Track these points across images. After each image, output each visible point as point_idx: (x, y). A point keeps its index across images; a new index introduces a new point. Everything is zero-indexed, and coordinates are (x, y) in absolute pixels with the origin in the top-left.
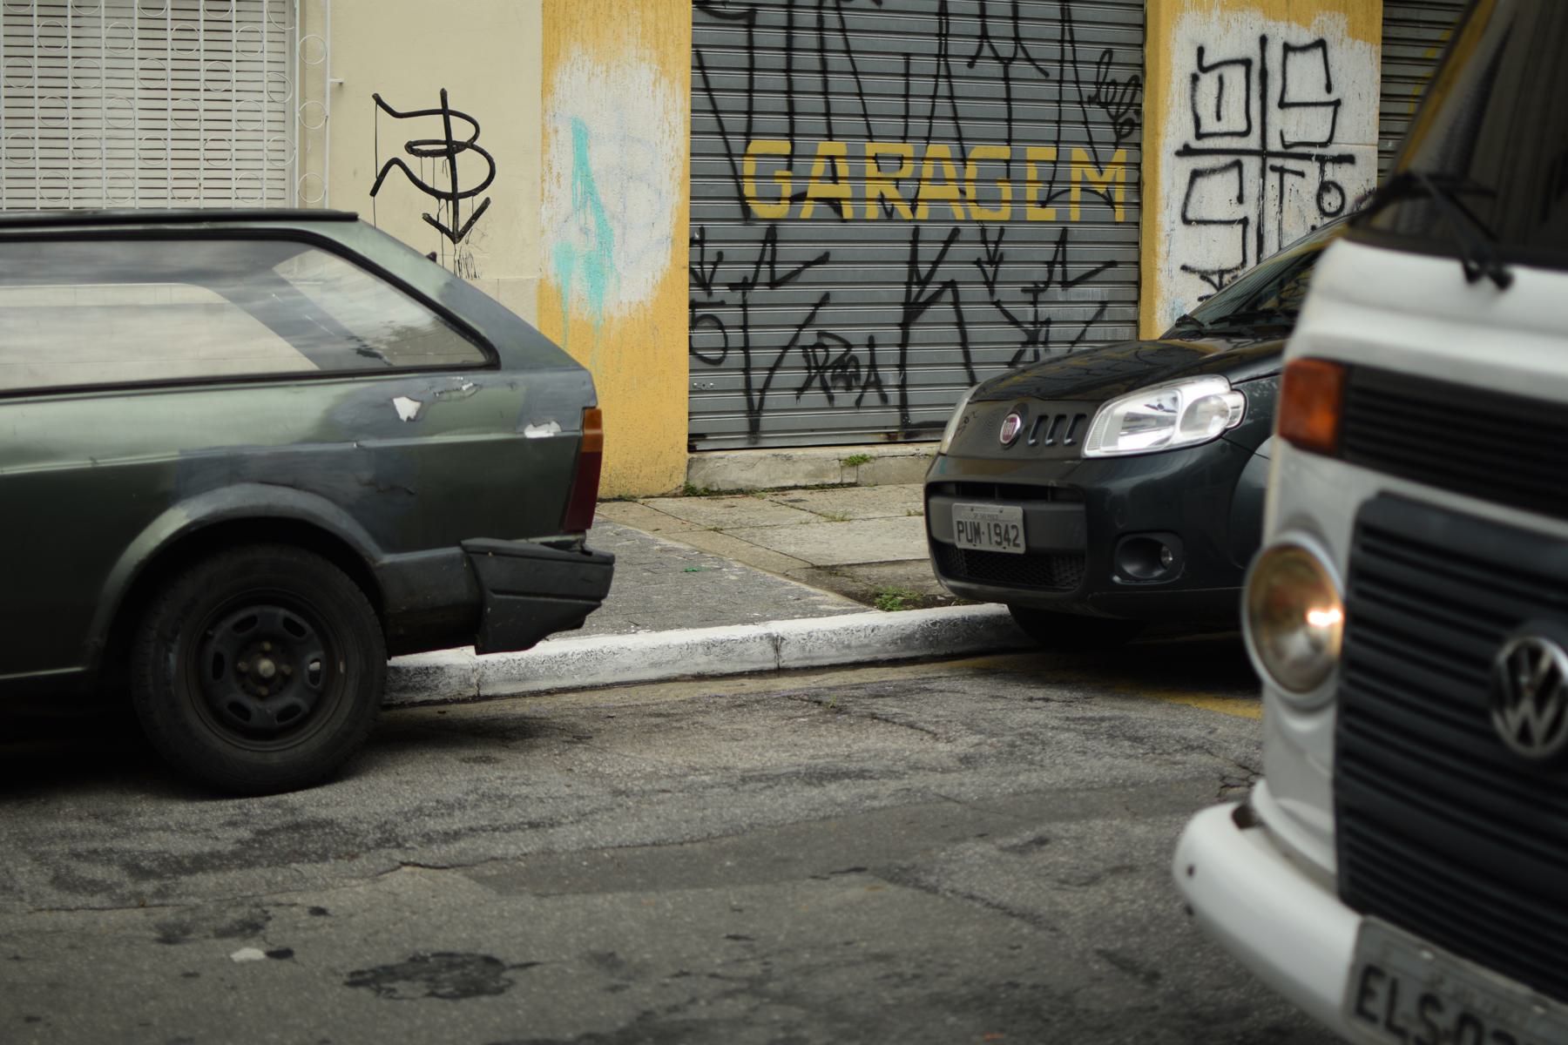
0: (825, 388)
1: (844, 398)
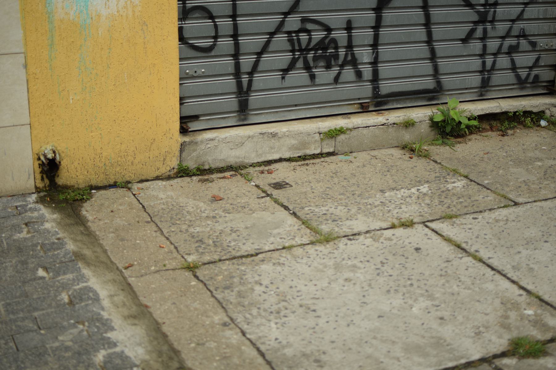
0: (307, 68)
1: (324, 75)
